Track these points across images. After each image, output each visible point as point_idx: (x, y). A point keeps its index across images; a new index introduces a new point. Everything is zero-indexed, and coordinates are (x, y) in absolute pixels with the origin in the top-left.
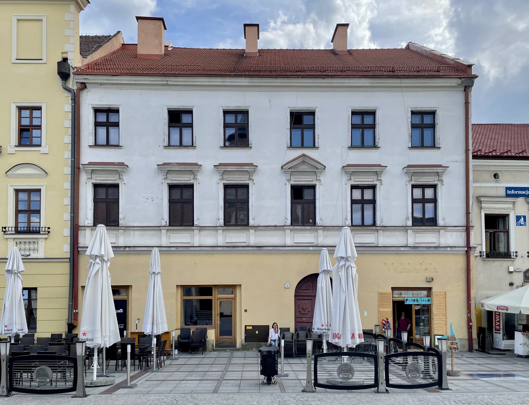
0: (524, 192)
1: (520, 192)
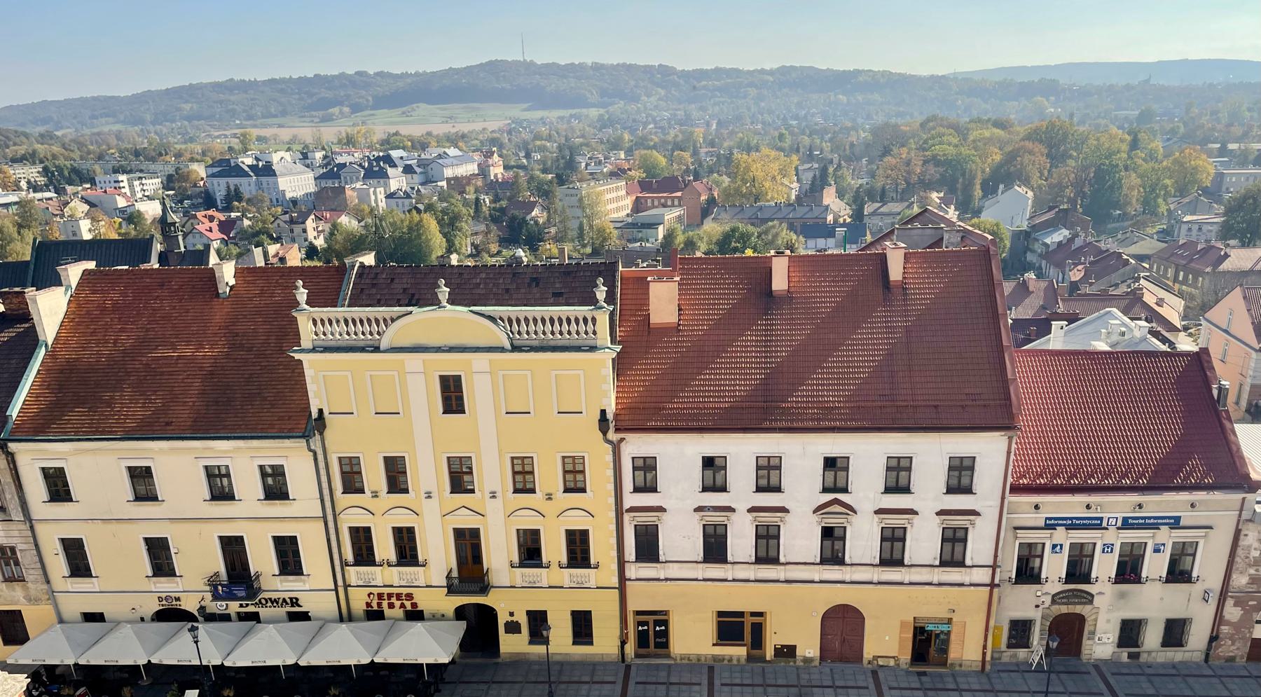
0: (1065, 522)
1: (1060, 522)
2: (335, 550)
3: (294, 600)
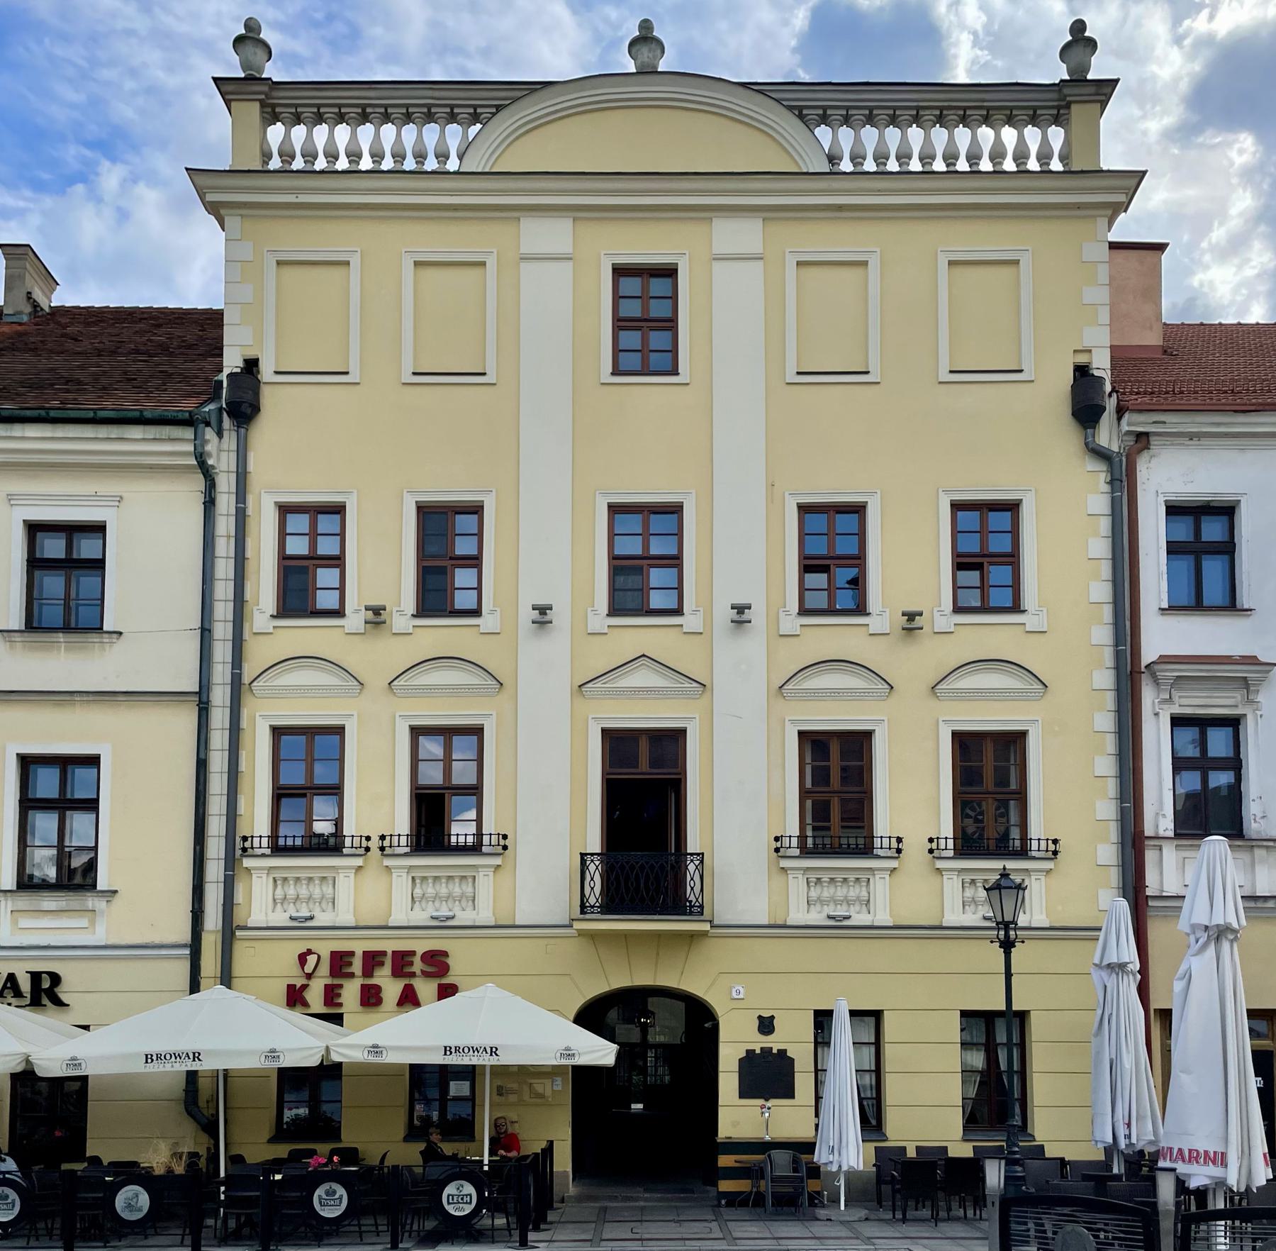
2: (217, 805)
3: (46, 984)
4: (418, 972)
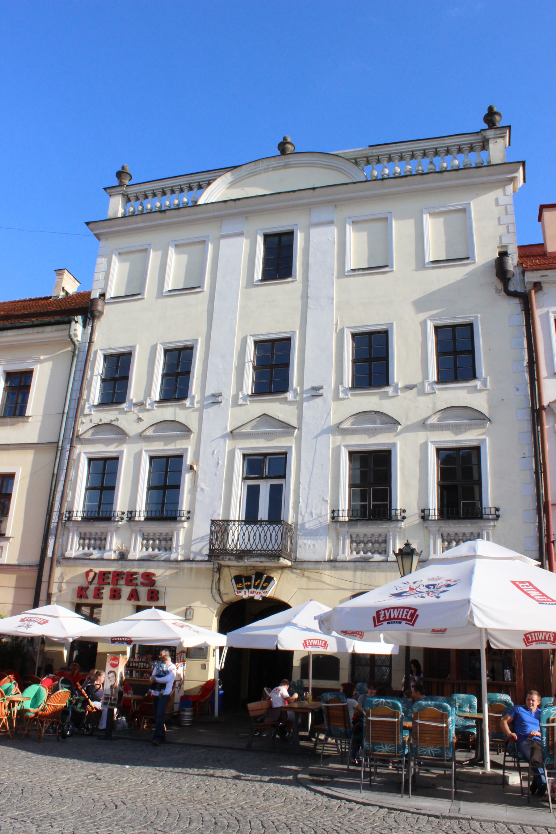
4: (139, 583)
